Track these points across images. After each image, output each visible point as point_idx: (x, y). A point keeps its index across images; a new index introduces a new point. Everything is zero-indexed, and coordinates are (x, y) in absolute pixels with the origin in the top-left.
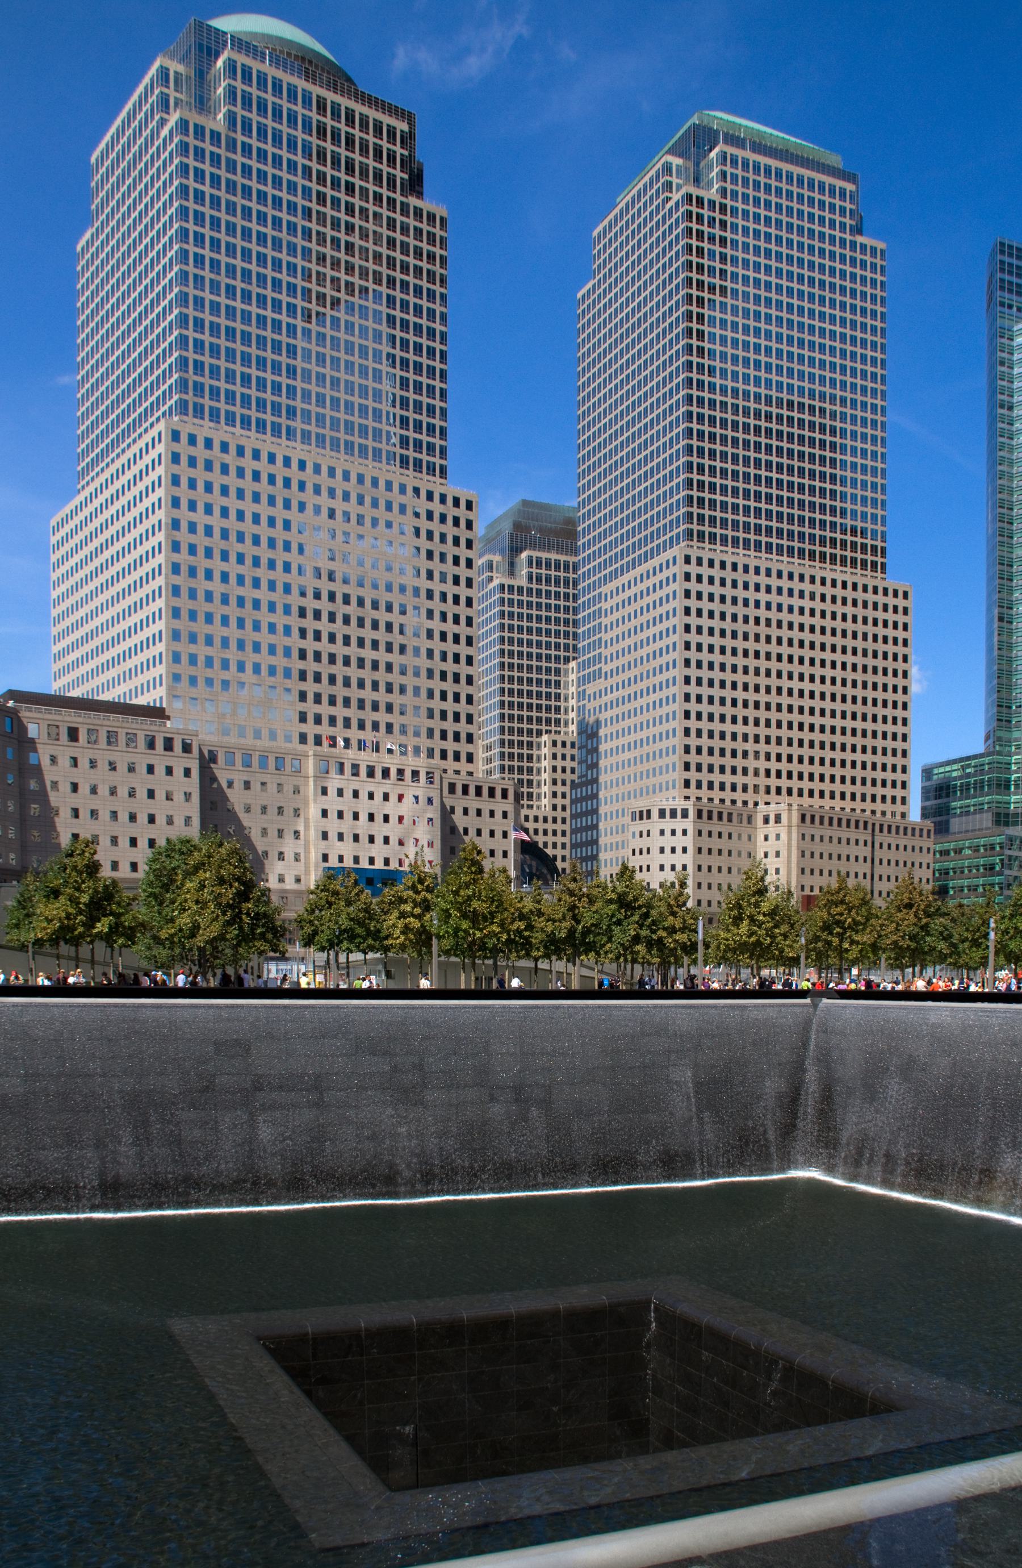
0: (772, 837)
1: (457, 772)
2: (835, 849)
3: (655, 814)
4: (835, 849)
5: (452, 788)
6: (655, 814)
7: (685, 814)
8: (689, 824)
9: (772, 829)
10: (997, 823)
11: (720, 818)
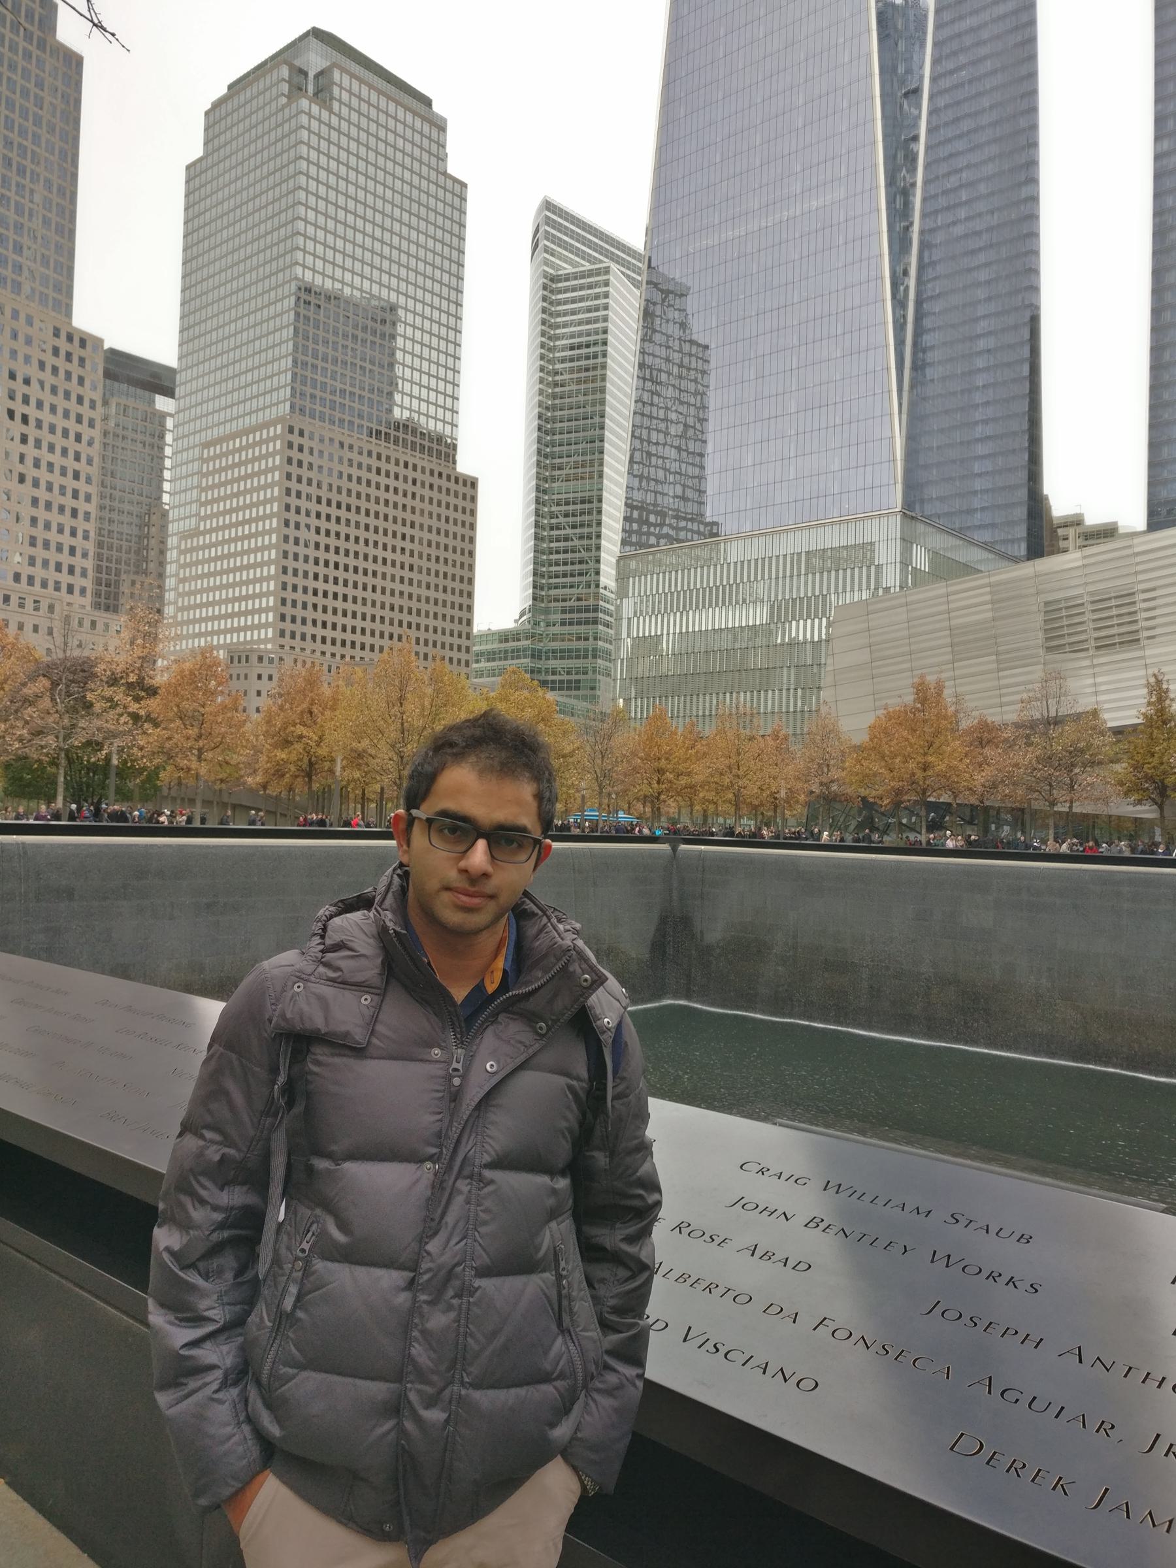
3: (254, 659)
6: (254, 659)
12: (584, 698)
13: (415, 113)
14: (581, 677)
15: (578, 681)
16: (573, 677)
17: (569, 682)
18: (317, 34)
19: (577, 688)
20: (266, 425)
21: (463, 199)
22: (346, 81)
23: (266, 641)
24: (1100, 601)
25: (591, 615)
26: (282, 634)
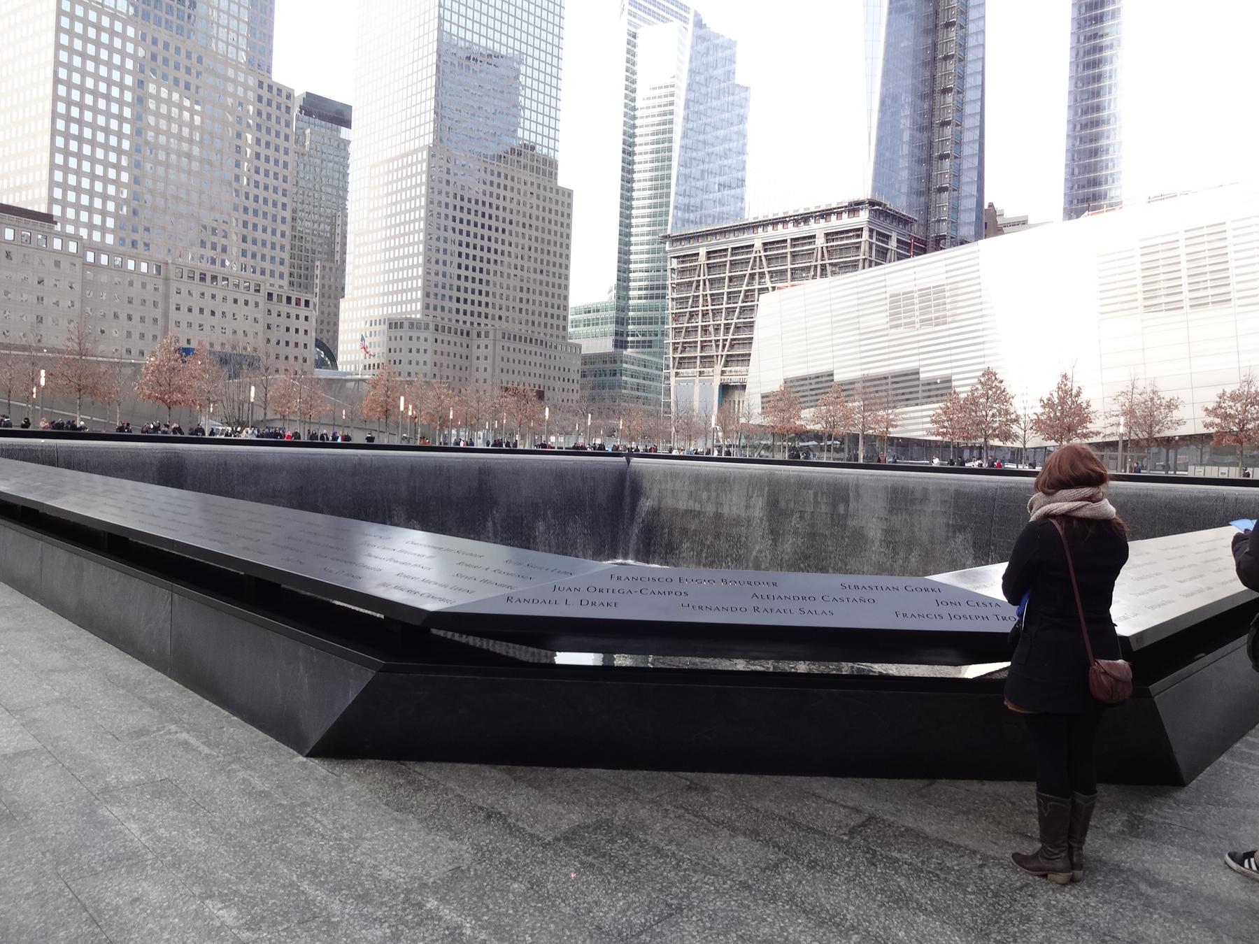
0: (482, 346)
1: (272, 285)
2: (522, 356)
3: (406, 325)
4: (522, 356)
5: (270, 295)
6: (406, 325)
7: (427, 327)
8: (430, 335)
9: (482, 342)
10: (616, 346)
11: (450, 332)
12: (654, 354)
14: (653, 338)
15: (650, 342)
16: (648, 338)
17: (644, 342)
19: (650, 347)
20: (416, 151)
23: (416, 312)
24: (924, 293)
25: (660, 292)
26: (427, 307)
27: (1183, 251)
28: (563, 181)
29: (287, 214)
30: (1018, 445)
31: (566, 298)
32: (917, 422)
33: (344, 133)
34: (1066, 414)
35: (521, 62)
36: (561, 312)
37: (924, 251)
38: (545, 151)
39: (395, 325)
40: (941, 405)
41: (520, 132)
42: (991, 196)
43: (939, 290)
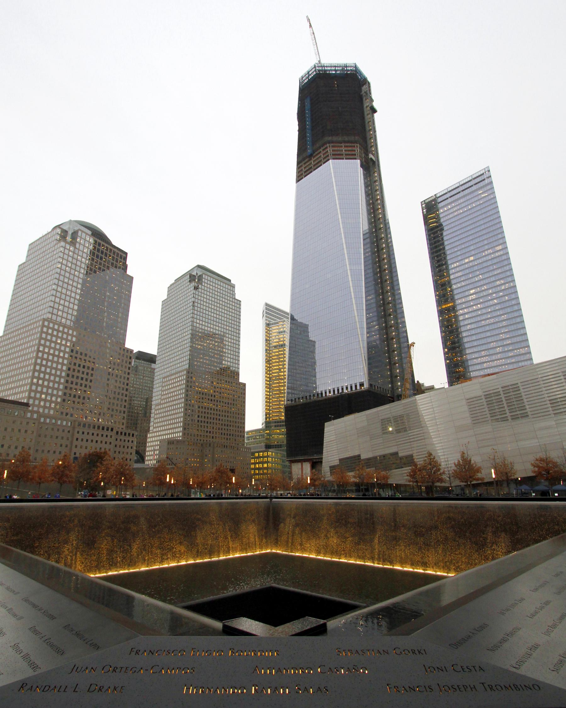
13: (226, 284)
18: (199, 266)
21: (240, 305)
22: (206, 277)
23: (180, 437)
27: (502, 396)
28: (241, 380)
29: (127, 398)
30: (447, 485)
31: (244, 428)
32: (400, 476)
33: (153, 366)
34: (466, 469)
35: (224, 336)
36: (242, 434)
37: (393, 401)
38: (234, 369)
39: (171, 442)
40: (410, 468)
41: (224, 362)
42: (418, 378)
43: (401, 417)
